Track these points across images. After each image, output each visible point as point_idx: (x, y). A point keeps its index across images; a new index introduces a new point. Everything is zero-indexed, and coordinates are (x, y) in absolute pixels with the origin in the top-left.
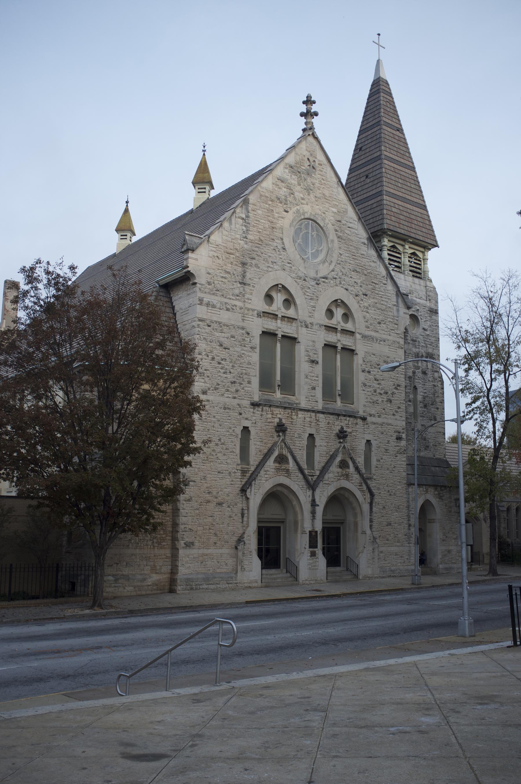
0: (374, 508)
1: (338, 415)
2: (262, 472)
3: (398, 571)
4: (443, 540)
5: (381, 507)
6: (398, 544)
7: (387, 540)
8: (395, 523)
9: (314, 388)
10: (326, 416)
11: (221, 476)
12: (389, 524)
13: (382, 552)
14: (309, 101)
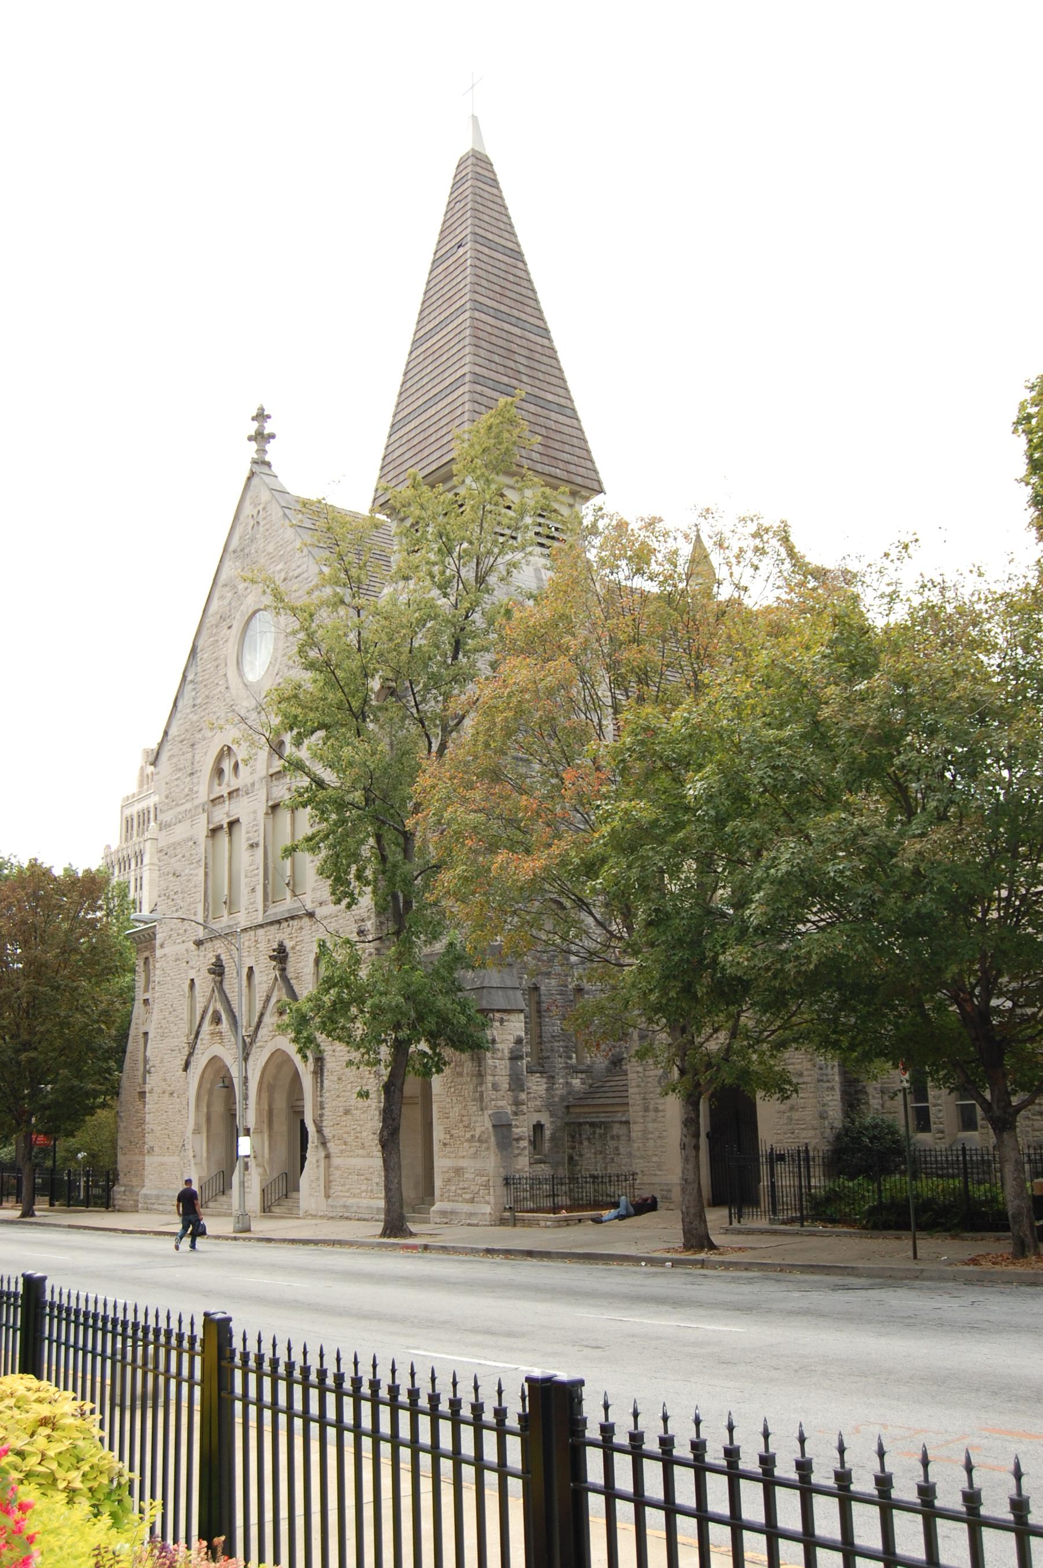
0: (326, 1083)
1: (279, 922)
2: (199, 1042)
3: (355, 1208)
4: (445, 1144)
5: (336, 1079)
6: (361, 1152)
7: (345, 1143)
8: (357, 1109)
9: (253, 890)
10: (265, 929)
11: (174, 1054)
12: (347, 1112)
13: (337, 1168)
14: (261, 416)
